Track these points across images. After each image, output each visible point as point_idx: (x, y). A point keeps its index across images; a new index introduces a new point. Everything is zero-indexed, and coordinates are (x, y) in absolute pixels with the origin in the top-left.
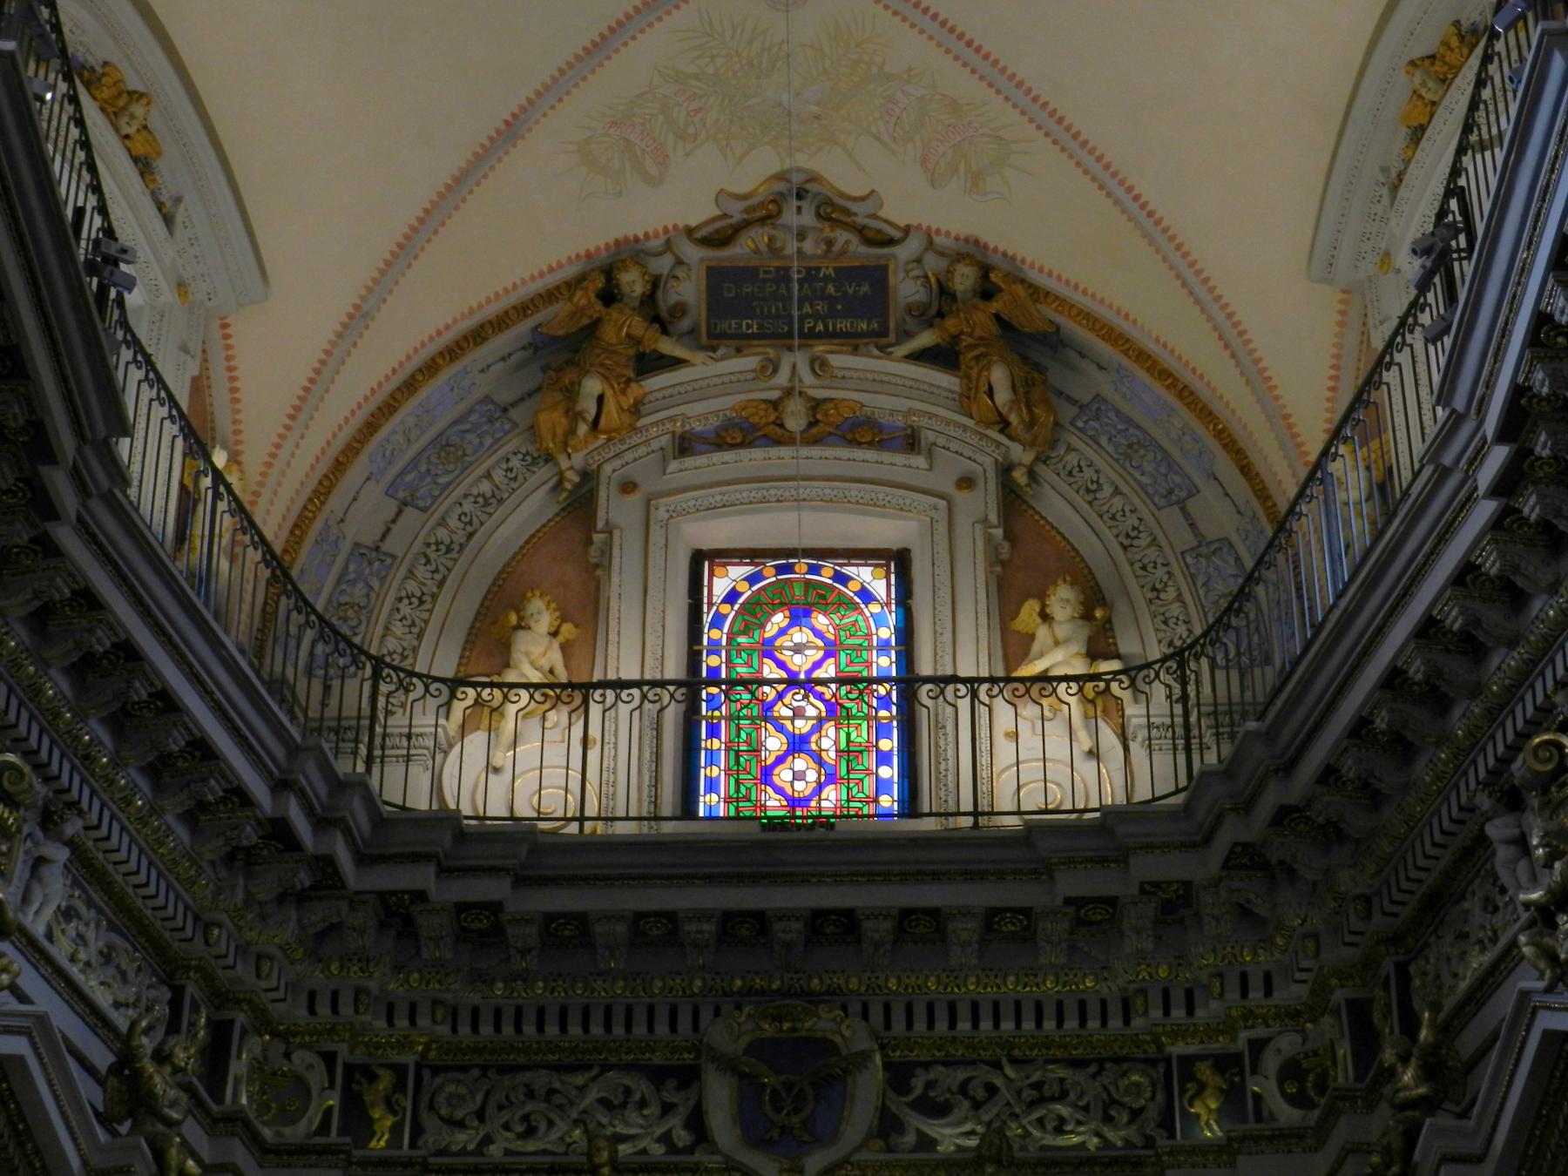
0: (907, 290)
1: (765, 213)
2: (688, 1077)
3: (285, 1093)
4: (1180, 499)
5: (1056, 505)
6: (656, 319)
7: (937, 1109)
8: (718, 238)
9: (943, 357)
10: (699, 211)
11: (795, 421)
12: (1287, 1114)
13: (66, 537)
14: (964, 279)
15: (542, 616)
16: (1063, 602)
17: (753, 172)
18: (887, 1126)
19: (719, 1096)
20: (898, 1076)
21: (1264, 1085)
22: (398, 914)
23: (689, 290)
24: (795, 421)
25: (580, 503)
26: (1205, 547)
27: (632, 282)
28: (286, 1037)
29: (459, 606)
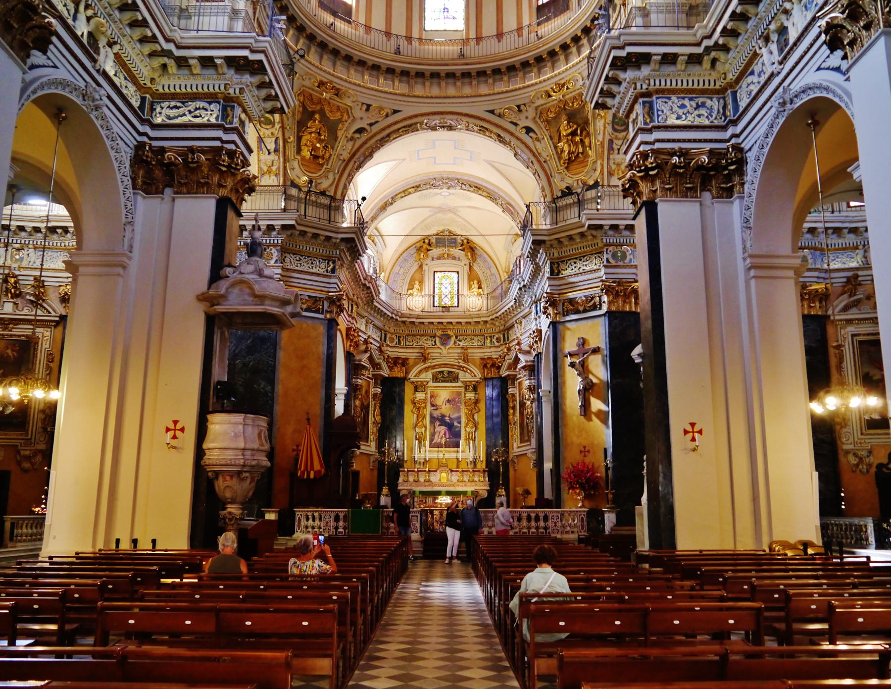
0: (459, 241)
1: (443, 231)
2: (434, 337)
3: (392, 340)
4: (489, 268)
5: (475, 267)
6: (429, 244)
7: (460, 341)
8: (437, 235)
9: (463, 250)
10: (435, 232)
11: (446, 256)
12: (497, 344)
13: (375, 304)
14: (465, 241)
15: (417, 283)
16: (475, 282)
17: (441, 229)
18: (455, 342)
19: (437, 339)
20: (456, 337)
21: (494, 340)
22: (404, 322)
23: (433, 240)
24: (446, 256)
25: (421, 266)
26: (492, 275)
27: (427, 241)
28: (392, 334)
29: (408, 279)
